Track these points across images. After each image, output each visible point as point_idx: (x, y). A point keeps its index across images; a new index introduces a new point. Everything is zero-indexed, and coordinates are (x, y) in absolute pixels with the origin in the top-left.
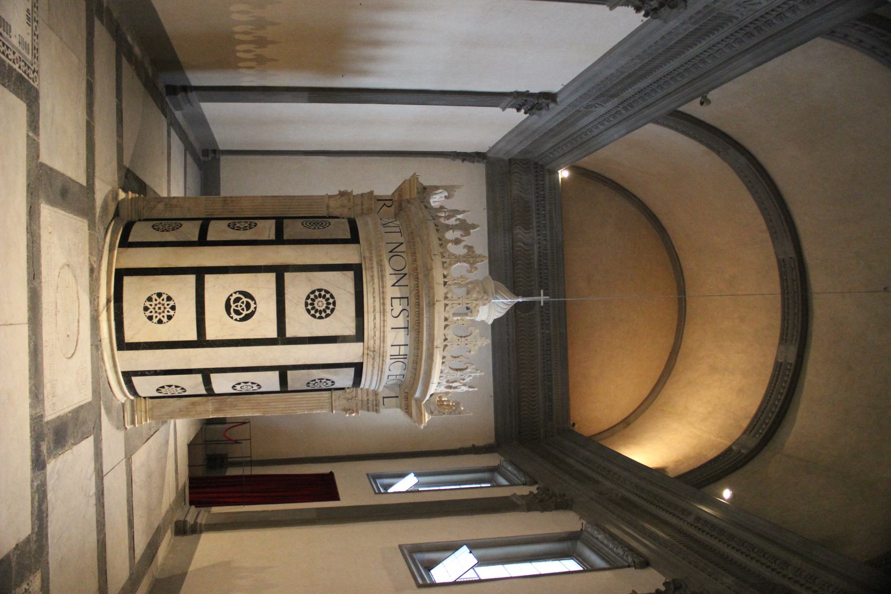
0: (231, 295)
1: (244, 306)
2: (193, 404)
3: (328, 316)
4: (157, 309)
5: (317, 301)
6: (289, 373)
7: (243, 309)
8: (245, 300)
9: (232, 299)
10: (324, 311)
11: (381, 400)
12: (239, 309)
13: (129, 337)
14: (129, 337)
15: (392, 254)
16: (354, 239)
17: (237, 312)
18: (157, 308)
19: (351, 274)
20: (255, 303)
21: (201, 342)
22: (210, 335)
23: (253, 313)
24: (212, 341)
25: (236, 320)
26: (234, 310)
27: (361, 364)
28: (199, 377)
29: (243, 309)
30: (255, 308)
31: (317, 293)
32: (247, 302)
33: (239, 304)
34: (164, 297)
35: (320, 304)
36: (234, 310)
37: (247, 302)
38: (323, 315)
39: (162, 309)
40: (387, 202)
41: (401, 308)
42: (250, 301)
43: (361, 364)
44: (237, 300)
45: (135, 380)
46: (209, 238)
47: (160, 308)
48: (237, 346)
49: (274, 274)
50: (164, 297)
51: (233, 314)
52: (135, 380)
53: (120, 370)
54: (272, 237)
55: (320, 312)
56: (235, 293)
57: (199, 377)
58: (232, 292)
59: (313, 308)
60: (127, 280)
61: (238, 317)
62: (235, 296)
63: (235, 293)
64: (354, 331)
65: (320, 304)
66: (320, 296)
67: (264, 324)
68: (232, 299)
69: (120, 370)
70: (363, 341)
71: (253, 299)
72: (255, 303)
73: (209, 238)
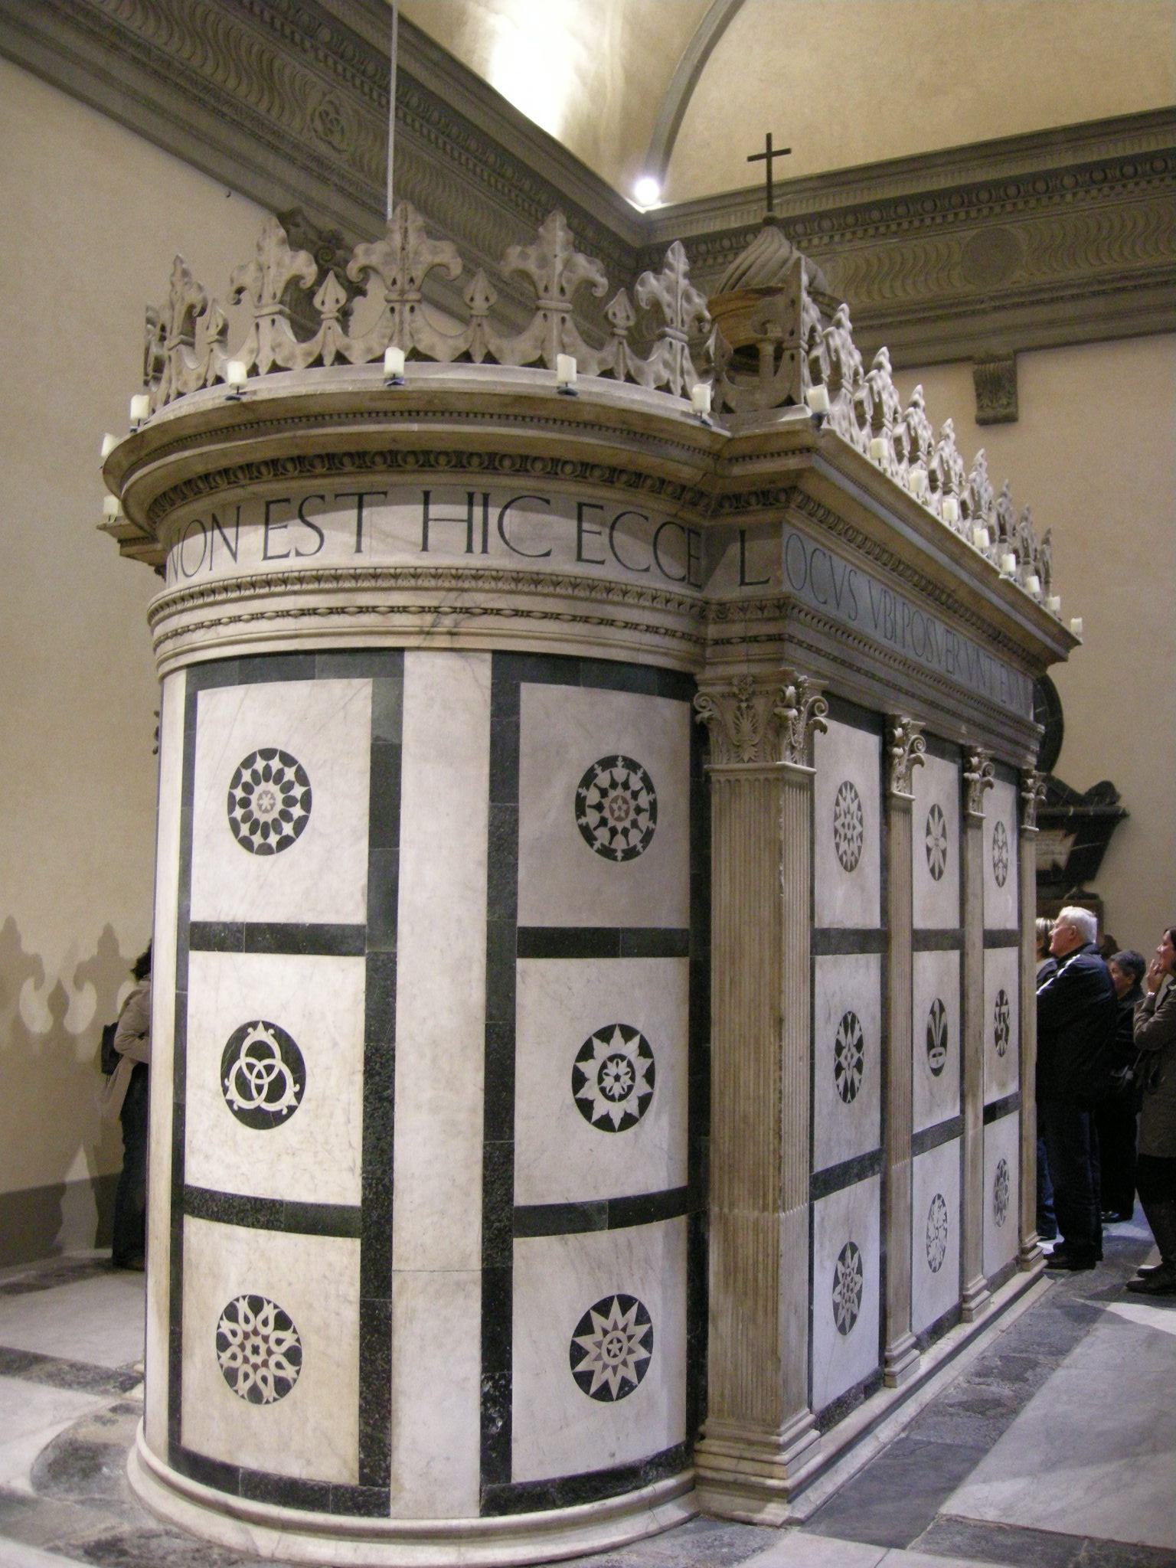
0: (230, 1103)
1: (260, 1066)
2: (730, 1271)
3: (302, 778)
5: (257, 815)
6: (525, 919)
7: (251, 1067)
8: (243, 1061)
9: (241, 1103)
10: (287, 787)
11: (748, 590)
13: (336, 1462)
14: (336, 1462)
17: (276, 1090)
21: (371, 1223)
22: (343, 1188)
23: (281, 1036)
24: (367, 1185)
25: (299, 1096)
27: (499, 656)
28: (526, 1250)
29: (269, 1069)
30: (268, 1026)
32: (251, 1052)
35: (266, 802)
38: (298, 791)
41: (298, 521)
42: (247, 1044)
43: (496, 653)
45: (525, 1469)
48: (391, 1101)
52: (525, 1469)
53: (473, 1520)
55: (289, 802)
56: (225, 1090)
57: (526, 1250)
59: (276, 826)
61: (291, 1088)
63: (225, 1090)
64: (357, 682)
65: (267, 800)
67: (318, 1000)
68: (241, 1103)
69: (473, 1520)
71: (241, 1034)
72: (254, 1025)
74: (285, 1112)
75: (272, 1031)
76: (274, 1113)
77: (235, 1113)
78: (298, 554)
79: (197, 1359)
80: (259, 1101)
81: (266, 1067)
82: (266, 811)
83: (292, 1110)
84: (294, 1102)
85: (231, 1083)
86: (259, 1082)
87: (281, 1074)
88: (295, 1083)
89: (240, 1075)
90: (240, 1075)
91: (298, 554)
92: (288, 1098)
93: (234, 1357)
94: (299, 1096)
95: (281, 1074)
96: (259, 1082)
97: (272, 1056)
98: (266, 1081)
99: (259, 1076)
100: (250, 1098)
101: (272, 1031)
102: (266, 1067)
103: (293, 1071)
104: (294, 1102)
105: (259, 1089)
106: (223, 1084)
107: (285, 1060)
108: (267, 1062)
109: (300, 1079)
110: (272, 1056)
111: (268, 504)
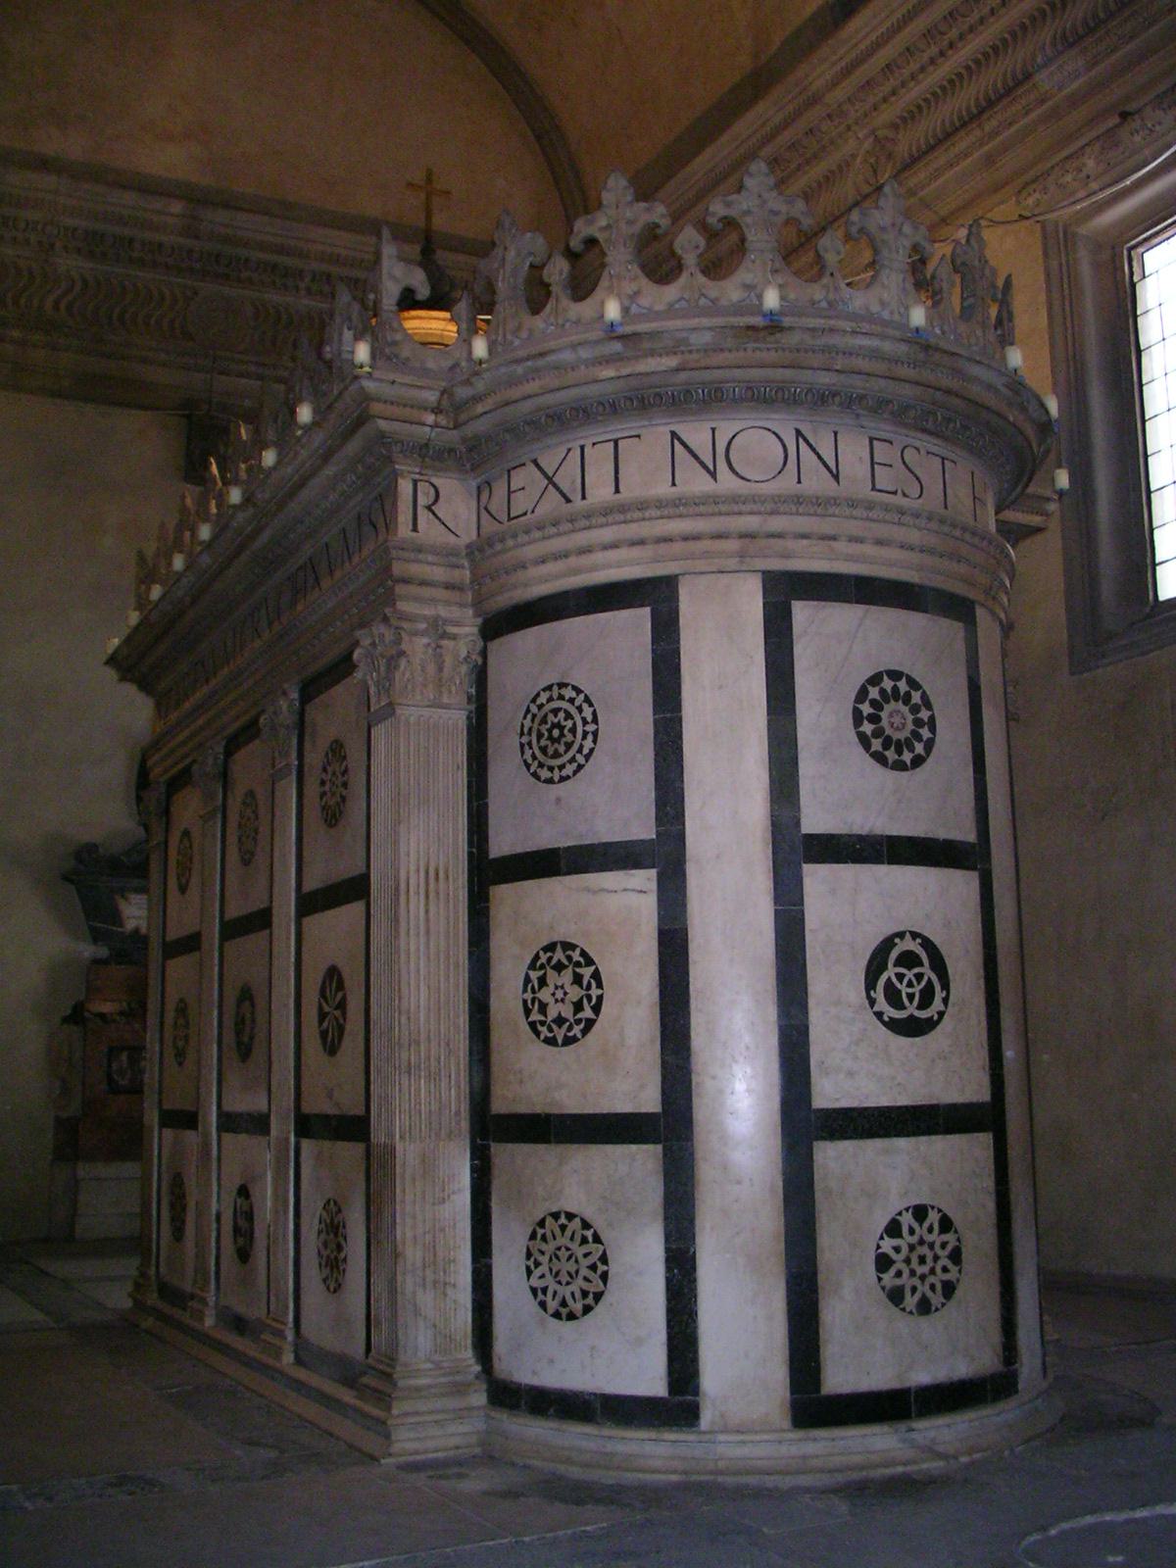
0: (879, 1015)
1: (910, 975)
4: (925, 1269)
8: (890, 972)
9: (891, 1013)
15: (722, 465)
16: (657, 597)
18: (921, 1270)
19: (802, 612)
23: (927, 944)
25: (945, 1001)
26: (920, 1007)
29: (919, 977)
30: (915, 935)
31: (867, 728)
32: (898, 963)
34: (887, 1245)
35: (897, 720)
36: (920, 1007)
37: (898, 963)
39: (924, 1250)
40: (422, 501)
42: (894, 954)
44: (893, 997)
46: (649, 1101)
47: (922, 1260)
49: (808, 869)
50: (887, 1245)
54: (645, 879)
56: (872, 1002)
60: (840, 1377)
61: (939, 994)
62: (882, 1004)
63: (872, 1002)
66: (874, 719)
68: (891, 1013)
70: (973, 602)
71: (888, 944)
72: (901, 935)
73: (649, 1101)
74: (936, 1017)
75: (919, 940)
77: (884, 1024)
78: (904, 495)
79: (847, 1292)
80: (911, 1009)
81: (915, 975)
82: (898, 729)
83: (941, 1014)
84: (942, 1008)
85: (879, 994)
86: (910, 990)
88: (942, 989)
91: (904, 495)
92: (937, 1004)
93: (899, 1274)
94: (945, 1001)
96: (910, 990)
98: (917, 989)
99: (910, 984)
100: (902, 1007)
101: (919, 940)
102: (915, 975)
105: (911, 997)
106: (869, 997)
107: (933, 968)
108: (916, 970)
109: (946, 986)
111: (871, 440)
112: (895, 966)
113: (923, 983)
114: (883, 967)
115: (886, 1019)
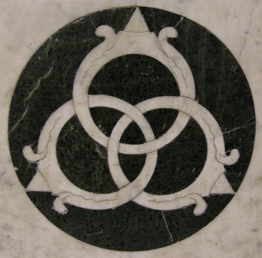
1: (133, 113)
8: (80, 104)
9: (72, 196)
12: (152, 147)
20: (118, 18)
23: (195, 41)
26: (156, 187)
29: (161, 120)
30: (156, 19)
32: (101, 84)
33: (113, 146)
36: (156, 187)
51: (191, 196)
56: (26, 172)
58: (17, 199)
63: (26, 172)
68: (72, 196)
71: (76, 38)
74: (201, 209)
76: (171, 214)
87: (193, 127)
88: (228, 147)
89: (72, 132)
90: (72, 132)
95: (193, 127)
97: (173, 89)
99: (133, 135)
102: (149, 115)
103: (224, 122)
104: (223, 187)
106: (17, 158)
107: (205, 97)
110: (173, 89)
112: (92, 91)
113: (172, 135)
114: (62, 94)
115: (59, 207)
